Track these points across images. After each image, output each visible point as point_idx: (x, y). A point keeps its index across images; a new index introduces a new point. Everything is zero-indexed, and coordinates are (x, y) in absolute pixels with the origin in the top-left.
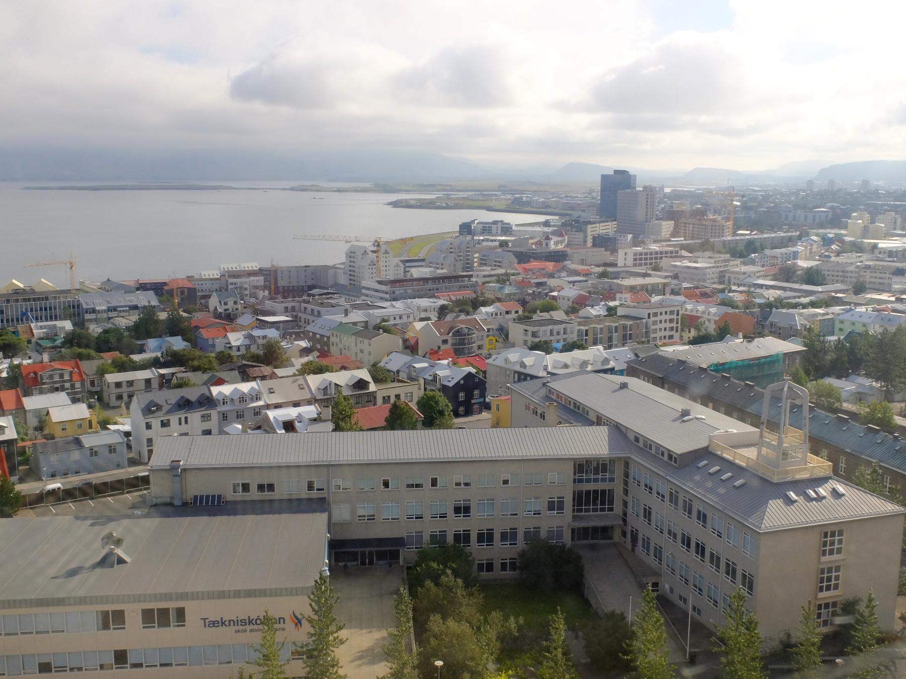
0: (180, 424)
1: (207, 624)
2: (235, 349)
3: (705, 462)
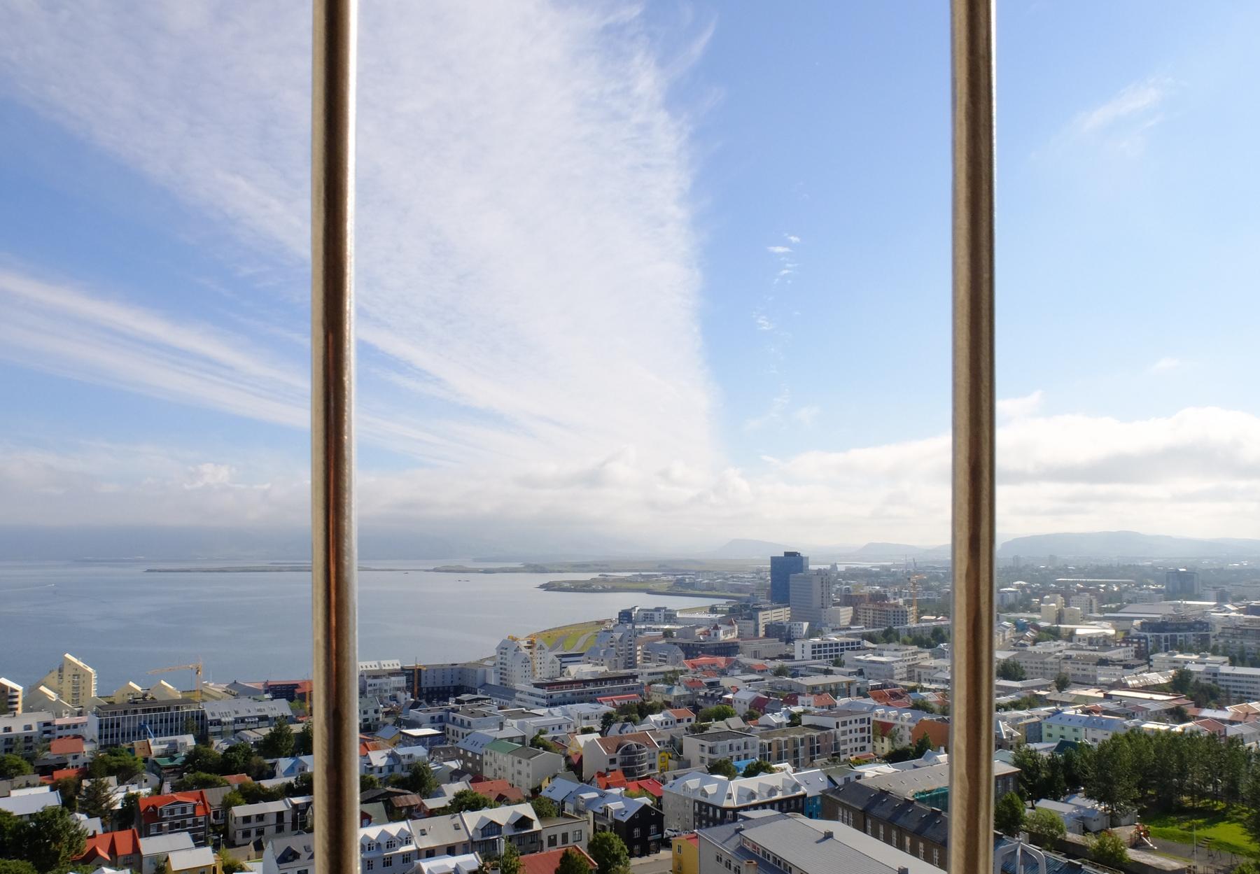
2: (376, 770)
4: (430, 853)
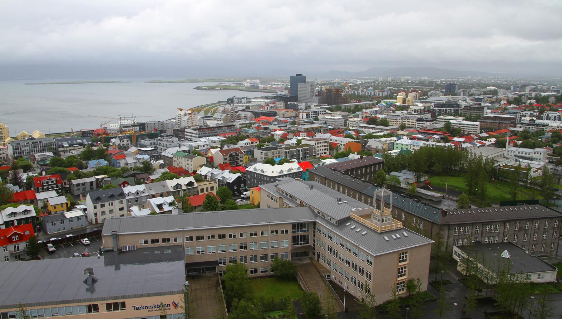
0: (109, 205)
1: (135, 308)
2: (129, 165)
3: (349, 223)
4: (153, 196)
